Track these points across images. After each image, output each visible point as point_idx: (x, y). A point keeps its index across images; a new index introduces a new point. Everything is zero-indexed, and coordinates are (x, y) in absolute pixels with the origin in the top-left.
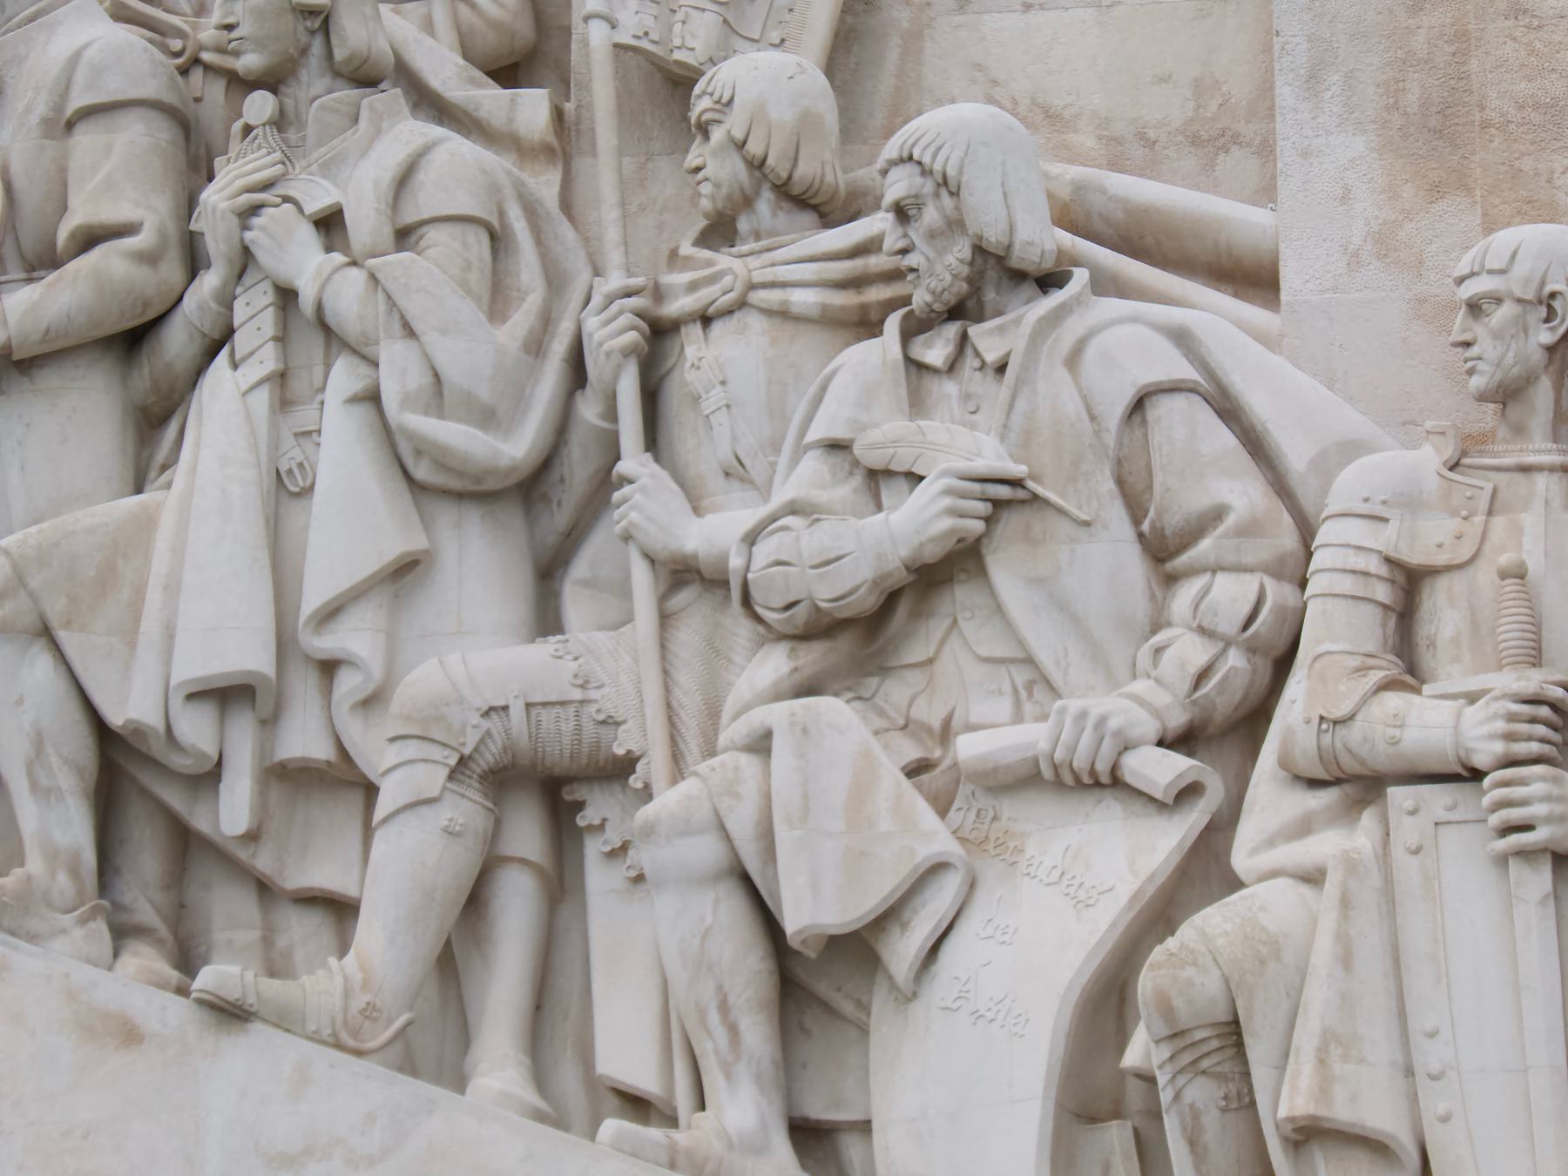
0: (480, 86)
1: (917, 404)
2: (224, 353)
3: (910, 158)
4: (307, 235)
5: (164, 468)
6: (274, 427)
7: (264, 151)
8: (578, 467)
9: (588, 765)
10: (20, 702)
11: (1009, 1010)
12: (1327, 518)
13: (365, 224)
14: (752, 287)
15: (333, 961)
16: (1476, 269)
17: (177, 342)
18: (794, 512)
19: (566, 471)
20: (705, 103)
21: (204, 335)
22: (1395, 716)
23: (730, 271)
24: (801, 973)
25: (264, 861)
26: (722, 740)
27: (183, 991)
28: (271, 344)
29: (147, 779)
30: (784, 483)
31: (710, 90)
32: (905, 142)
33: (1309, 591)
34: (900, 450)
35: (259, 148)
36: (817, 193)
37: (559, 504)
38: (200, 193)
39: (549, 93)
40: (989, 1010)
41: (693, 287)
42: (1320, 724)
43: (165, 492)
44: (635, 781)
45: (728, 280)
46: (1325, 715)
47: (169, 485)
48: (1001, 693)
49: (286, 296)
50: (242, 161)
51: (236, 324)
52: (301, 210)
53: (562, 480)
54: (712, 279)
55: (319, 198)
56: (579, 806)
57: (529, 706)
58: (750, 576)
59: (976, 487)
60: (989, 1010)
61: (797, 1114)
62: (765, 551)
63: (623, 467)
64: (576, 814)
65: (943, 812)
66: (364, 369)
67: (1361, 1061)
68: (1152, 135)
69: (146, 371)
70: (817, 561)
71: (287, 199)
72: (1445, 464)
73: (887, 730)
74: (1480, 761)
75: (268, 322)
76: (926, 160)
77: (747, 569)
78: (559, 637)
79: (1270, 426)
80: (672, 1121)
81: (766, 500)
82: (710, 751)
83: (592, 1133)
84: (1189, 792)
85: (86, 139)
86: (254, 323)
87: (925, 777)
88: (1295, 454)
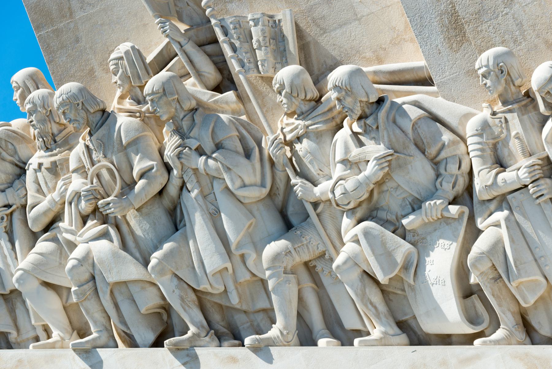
0: (215, 96)
1: (361, 144)
2: (184, 189)
3: (336, 86)
4: (194, 155)
5: (181, 221)
6: (205, 203)
7: (175, 136)
8: (281, 185)
9: (313, 256)
10: (174, 291)
11: (439, 280)
12: (468, 137)
13: (208, 146)
14: (307, 127)
15: (273, 325)
16: (480, 66)
17: (173, 190)
18: (341, 179)
19: (278, 186)
20: (278, 86)
21: (178, 186)
22: (503, 180)
23: (299, 124)
24: (385, 288)
25: (244, 308)
26: (345, 240)
27: (243, 346)
28: (196, 183)
29: (208, 298)
30: (334, 174)
31: (277, 82)
32: (333, 82)
33: (471, 156)
34: (360, 156)
35: (174, 136)
36: (313, 97)
37: (279, 194)
38: (164, 152)
39: (233, 92)
40: (434, 281)
41: (292, 131)
42: (486, 187)
43: (184, 228)
44: (327, 256)
45: (300, 127)
46: (486, 185)
47: (185, 225)
48: (407, 205)
49: (196, 171)
50: (170, 142)
51: (186, 182)
52: (190, 148)
53: (278, 189)
54: (296, 128)
55: (194, 144)
56: (315, 267)
57: (295, 249)
58: (336, 199)
59: (384, 160)
60: (434, 281)
61: (397, 321)
62: (338, 192)
63: (293, 181)
64: (315, 268)
65: (404, 239)
66: (221, 181)
67: (525, 263)
68: (383, 46)
69: (167, 199)
70: (352, 190)
71: (186, 147)
72: (491, 114)
73: (383, 224)
74: (527, 184)
75: (193, 178)
76: (340, 85)
77: (335, 197)
78: (293, 229)
79: (446, 118)
80: (368, 334)
81: (331, 178)
82: (344, 244)
83: (352, 344)
84: (462, 214)
85: (129, 150)
86: (190, 180)
87: (397, 232)
88: (453, 121)
